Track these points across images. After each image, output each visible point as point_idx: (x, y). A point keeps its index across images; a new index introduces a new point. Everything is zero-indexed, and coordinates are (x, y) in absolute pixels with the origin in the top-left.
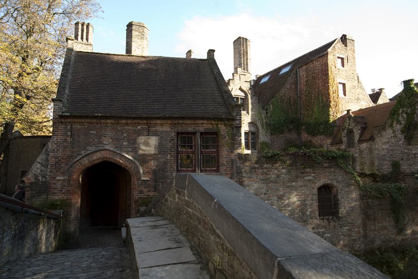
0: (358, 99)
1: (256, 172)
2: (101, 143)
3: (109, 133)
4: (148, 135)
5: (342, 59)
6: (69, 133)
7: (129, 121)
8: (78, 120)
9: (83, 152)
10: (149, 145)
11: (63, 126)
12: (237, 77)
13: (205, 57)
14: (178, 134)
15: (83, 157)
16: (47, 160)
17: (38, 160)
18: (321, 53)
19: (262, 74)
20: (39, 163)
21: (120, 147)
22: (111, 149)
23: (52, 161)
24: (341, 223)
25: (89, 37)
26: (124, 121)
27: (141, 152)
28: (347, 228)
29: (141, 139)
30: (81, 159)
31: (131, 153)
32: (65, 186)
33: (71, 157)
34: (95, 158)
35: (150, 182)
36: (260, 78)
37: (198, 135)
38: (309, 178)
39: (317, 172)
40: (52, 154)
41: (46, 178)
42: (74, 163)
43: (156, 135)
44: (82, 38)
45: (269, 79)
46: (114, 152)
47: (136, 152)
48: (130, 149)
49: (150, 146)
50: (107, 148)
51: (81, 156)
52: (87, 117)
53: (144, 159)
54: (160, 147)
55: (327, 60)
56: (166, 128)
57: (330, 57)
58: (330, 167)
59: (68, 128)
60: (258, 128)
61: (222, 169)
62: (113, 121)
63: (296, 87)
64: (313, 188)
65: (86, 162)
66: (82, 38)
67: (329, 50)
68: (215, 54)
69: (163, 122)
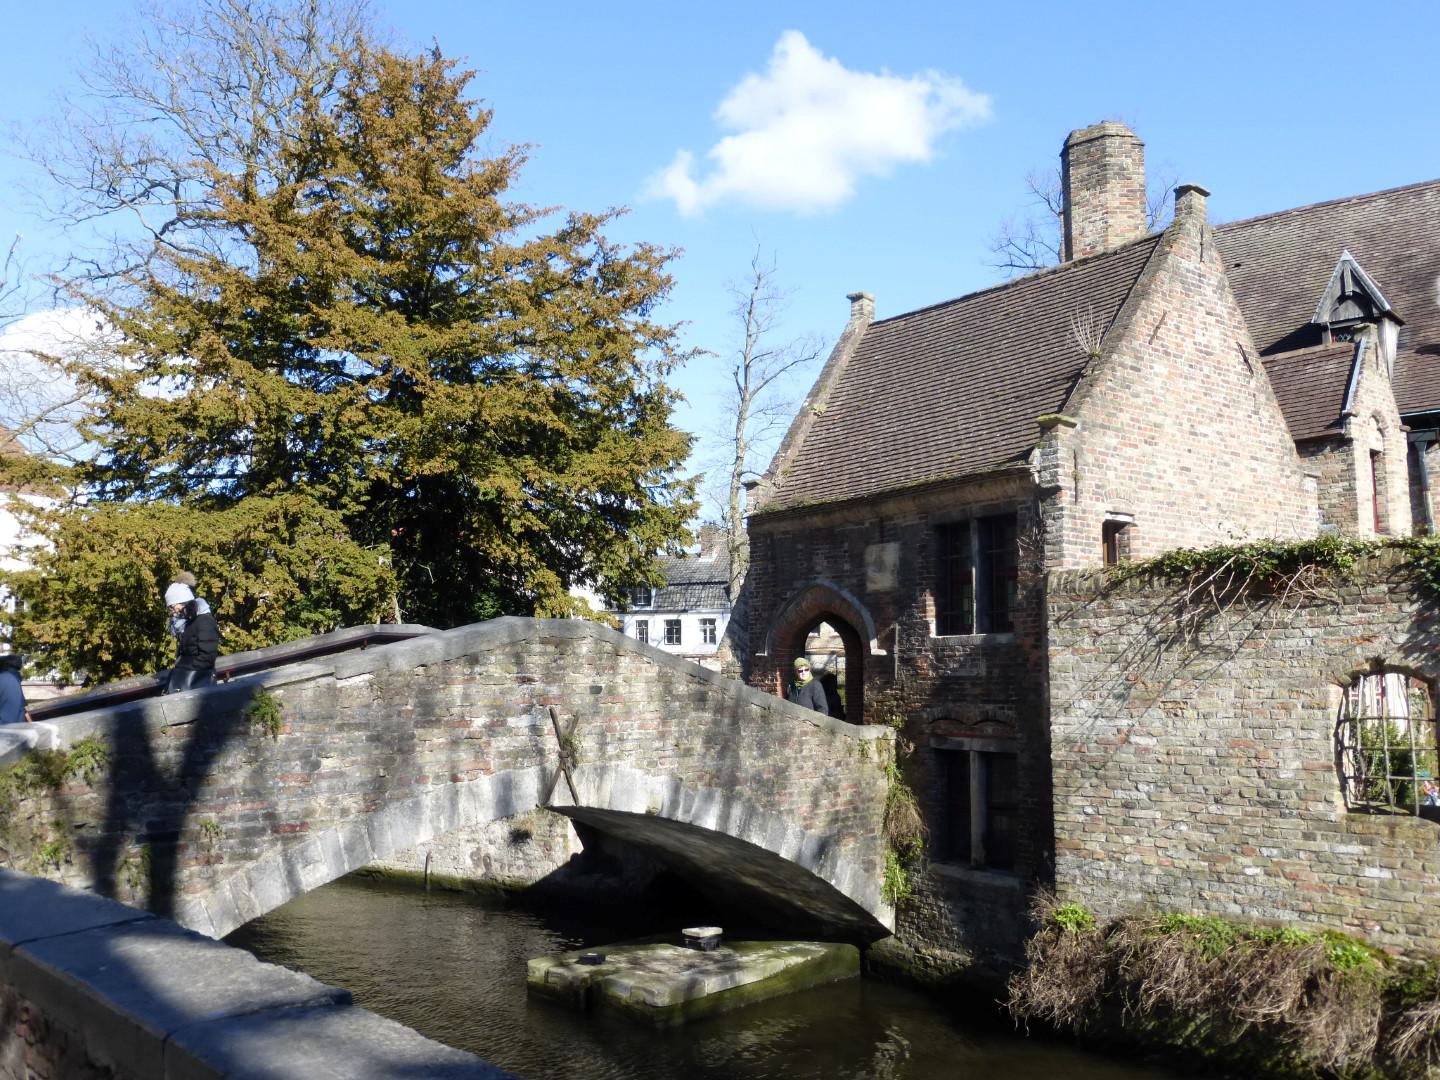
2: (811, 570)
4: (882, 542)
22: (827, 583)
27: (871, 587)
29: (872, 553)
37: (974, 525)
43: (894, 538)
48: (854, 581)
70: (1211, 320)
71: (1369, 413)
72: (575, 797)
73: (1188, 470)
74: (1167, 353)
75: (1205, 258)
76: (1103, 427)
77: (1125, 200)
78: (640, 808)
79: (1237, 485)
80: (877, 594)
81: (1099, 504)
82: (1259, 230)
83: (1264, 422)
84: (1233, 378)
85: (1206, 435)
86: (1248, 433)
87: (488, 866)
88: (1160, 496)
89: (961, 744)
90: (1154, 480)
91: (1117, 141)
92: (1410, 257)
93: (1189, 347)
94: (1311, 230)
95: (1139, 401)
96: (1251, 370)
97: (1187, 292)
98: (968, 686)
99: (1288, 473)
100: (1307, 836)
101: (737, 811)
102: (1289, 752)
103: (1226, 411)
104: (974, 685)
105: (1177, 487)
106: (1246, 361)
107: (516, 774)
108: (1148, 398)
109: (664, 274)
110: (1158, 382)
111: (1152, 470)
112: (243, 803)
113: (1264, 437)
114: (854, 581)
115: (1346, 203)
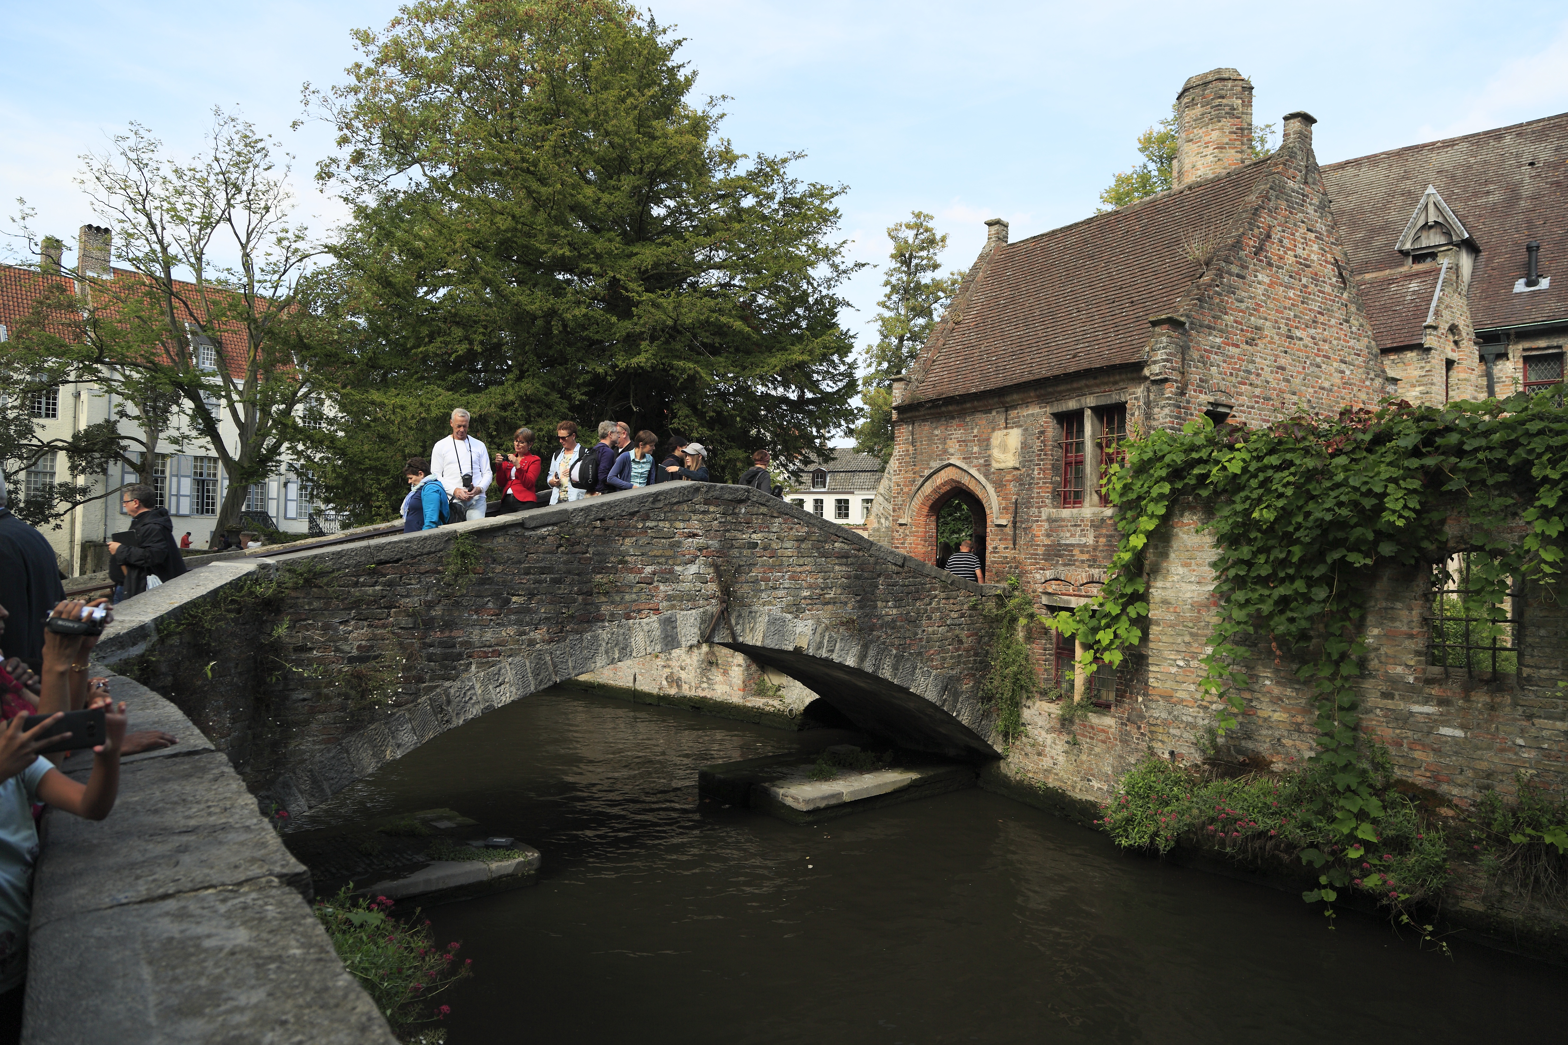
2: (945, 451)
22: (958, 463)
27: (995, 465)
29: (997, 437)
37: (1088, 413)
53: (999, 480)
70: (1312, 236)
71: (1447, 326)
72: (734, 635)
73: (1283, 369)
74: (1270, 264)
75: (1310, 180)
76: (1209, 327)
77: (1234, 136)
78: (791, 648)
79: (1327, 385)
81: (1202, 396)
82: (1350, 171)
83: (1354, 329)
84: (1328, 289)
85: (1301, 339)
86: (1339, 339)
87: (679, 687)
88: (1257, 391)
89: (1069, 602)
90: (1253, 377)
91: (1230, 84)
92: (1488, 192)
93: (1290, 259)
94: (1397, 171)
95: (1243, 306)
96: (1344, 283)
97: (1290, 208)
98: (1076, 552)
99: (1372, 375)
100: (1386, 695)
101: (871, 653)
103: (1321, 318)
104: (1082, 552)
105: (1274, 384)
106: (1341, 274)
107: (680, 615)
108: (1250, 303)
109: (831, 208)
110: (1260, 290)
111: (1251, 367)
112: (442, 632)
113: (1352, 342)
114: (982, 461)
115: (1432, 147)
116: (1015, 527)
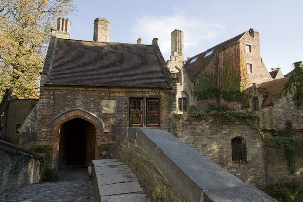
0: (261, 75)
1: (186, 127)
2: (75, 105)
3: (81, 98)
4: (109, 100)
5: (250, 46)
6: (52, 97)
7: (95, 89)
8: (58, 88)
9: (61, 111)
10: (109, 107)
11: (47, 92)
12: (173, 59)
13: (151, 44)
14: (130, 99)
15: (61, 115)
16: (35, 116)
17: (29, 116)
18: (235, 41)
19: (191, 57)
20: (30, 118)
21: (88, 108)
22: (82, 109)
23: (39, 117)
24: (249, 165)
25: (67, 29)
26: (91, 89)
27: (103, 112)
28: (253, 169)
29: (104, 103)
30: (59, 116)
31: (96, 113)
32: (48, 135)
33: (53, 115)
34: (70, 115)
35: (109, 134)
36: (190, 59)
37: (145, 100)
38: (225, 132)
39: (231, 128)
40: (39, 112)
41: (34, 130)
42: (55, 119)
43: (114, 99)
44: (62, 29)
45: (197, 60)
46: (84, 111)
47: (100, 112)
48: (96, 110)
49: (110, 108)
50: (79, 108)
51: (59, 114)
52: (65, 86)
53: (105, 117)
54: (118, 109)
55: (239, 47)
56: (122, 95)
57: (241, 45)
58: (241, 124)
59: (51, 93)
60: (188, 96)
61: (162, 125)
62: (83, 89)
63: (216, 66)
64: (228, 140)
65: (64, 119)
66: (62, 29)
67: (241, 40)
68: (158, 41)
69: (120, 90)
80: (105, 114)
102: (225, 153)
116: (114, 133)
